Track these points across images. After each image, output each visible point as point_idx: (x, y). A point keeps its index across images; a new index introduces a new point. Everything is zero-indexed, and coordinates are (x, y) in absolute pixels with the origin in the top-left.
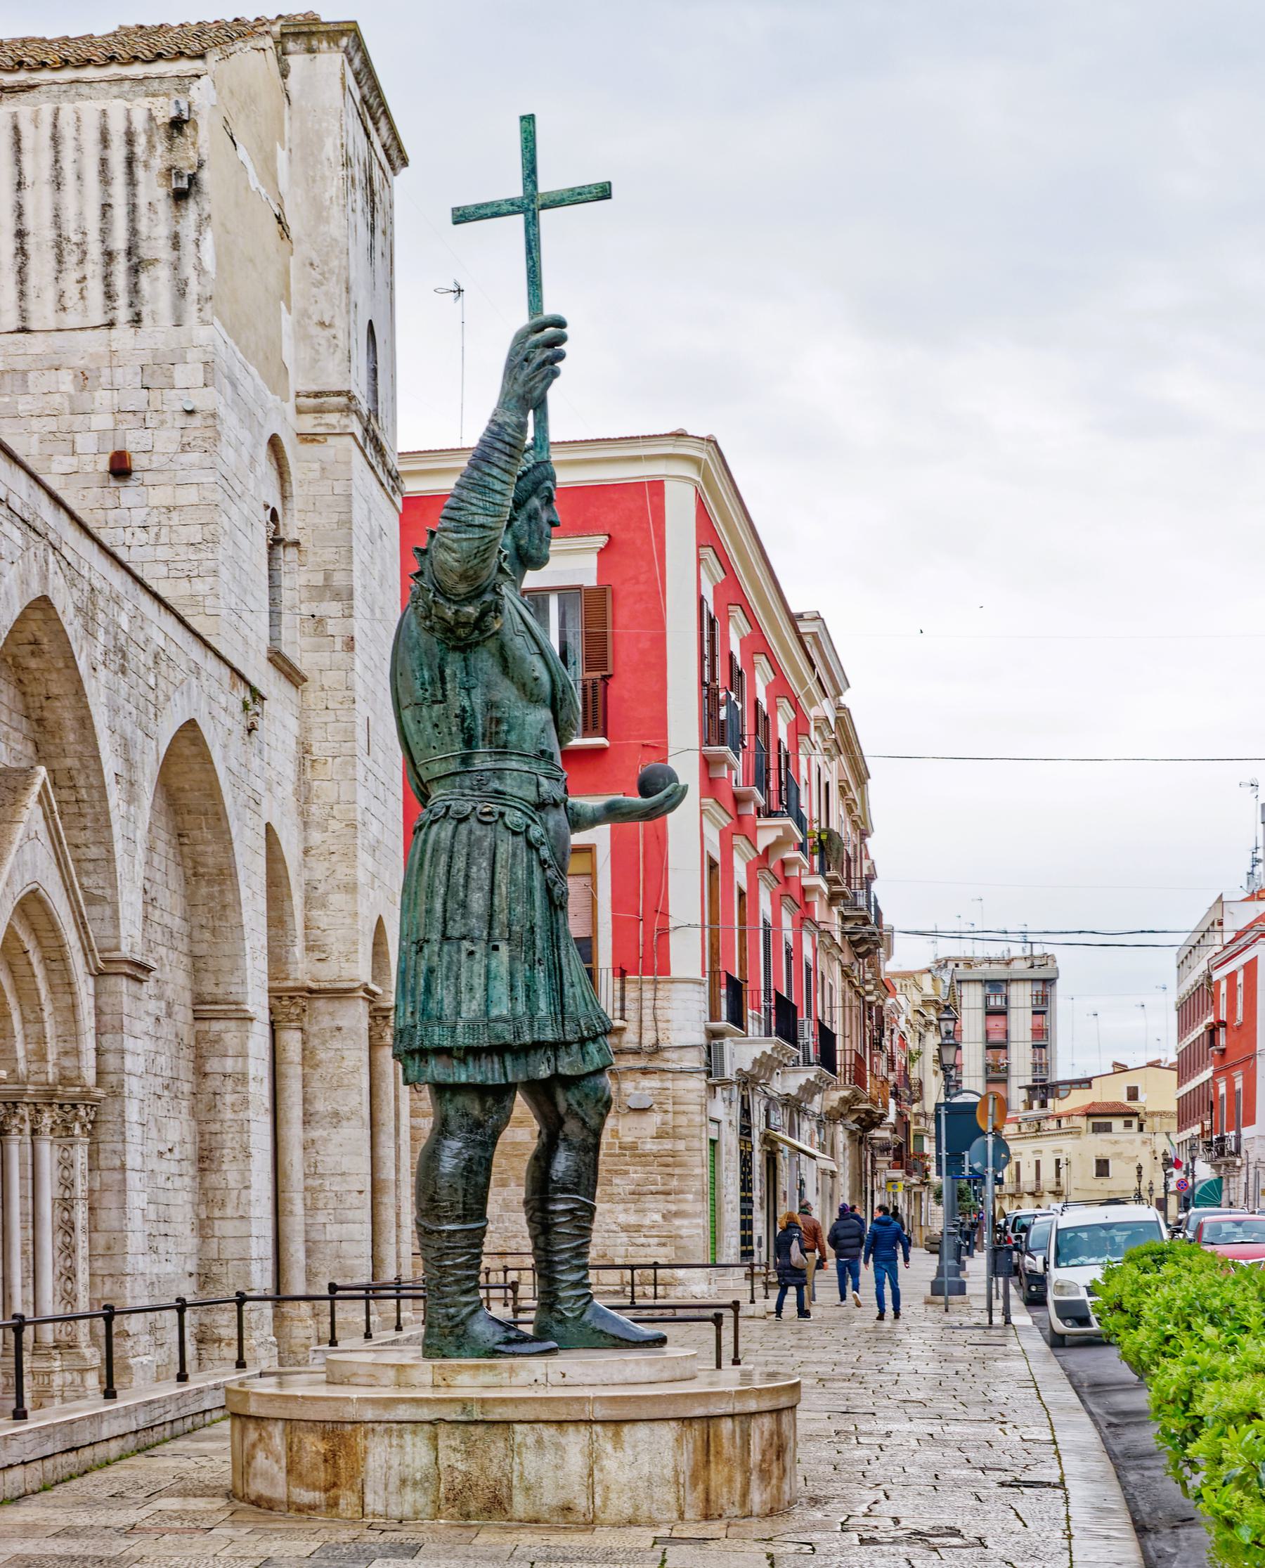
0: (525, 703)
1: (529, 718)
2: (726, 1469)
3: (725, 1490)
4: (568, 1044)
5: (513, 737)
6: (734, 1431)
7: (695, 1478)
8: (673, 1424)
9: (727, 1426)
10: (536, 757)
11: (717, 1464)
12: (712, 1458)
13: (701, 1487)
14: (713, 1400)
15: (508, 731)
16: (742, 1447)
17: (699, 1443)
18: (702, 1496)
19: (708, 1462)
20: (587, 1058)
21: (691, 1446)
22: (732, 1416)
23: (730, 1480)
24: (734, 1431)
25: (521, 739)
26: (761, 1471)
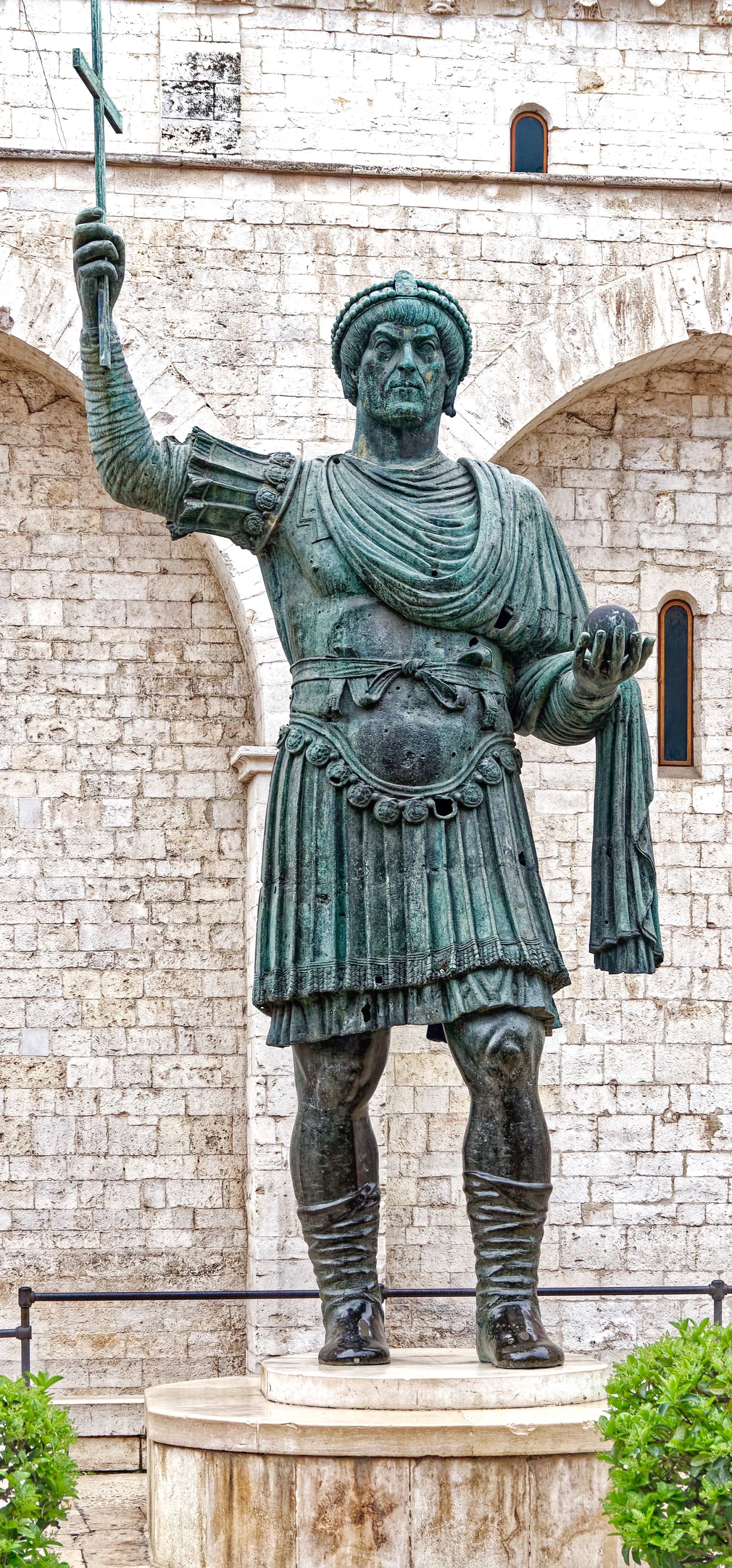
0: (319, 600)
1: (319, 617)
2: (254, 1521)
3: (252, 1547)
4: (420, 989)
5: (307, 643)
6: (266, 1476)
7: (216, 1524)
8: (198, 1455)
9: (255, 1467)
10: (330, 659)
11: (242, 1512)
12: (235, 1504)
13: (222, 1537)
14: (231, 1431)
15: (303, 637)
16: (280, 1497)
17: (221, 1483)
18: (223, 1549)
19: (230, 1508)
20: (452, 1003)
21: (213, 1484)
22: (263, 1455)
23: (259, 1535)
24: (266, 1476)
25: (314, 643)
26: (315, 1531)
